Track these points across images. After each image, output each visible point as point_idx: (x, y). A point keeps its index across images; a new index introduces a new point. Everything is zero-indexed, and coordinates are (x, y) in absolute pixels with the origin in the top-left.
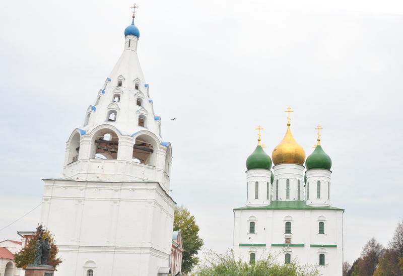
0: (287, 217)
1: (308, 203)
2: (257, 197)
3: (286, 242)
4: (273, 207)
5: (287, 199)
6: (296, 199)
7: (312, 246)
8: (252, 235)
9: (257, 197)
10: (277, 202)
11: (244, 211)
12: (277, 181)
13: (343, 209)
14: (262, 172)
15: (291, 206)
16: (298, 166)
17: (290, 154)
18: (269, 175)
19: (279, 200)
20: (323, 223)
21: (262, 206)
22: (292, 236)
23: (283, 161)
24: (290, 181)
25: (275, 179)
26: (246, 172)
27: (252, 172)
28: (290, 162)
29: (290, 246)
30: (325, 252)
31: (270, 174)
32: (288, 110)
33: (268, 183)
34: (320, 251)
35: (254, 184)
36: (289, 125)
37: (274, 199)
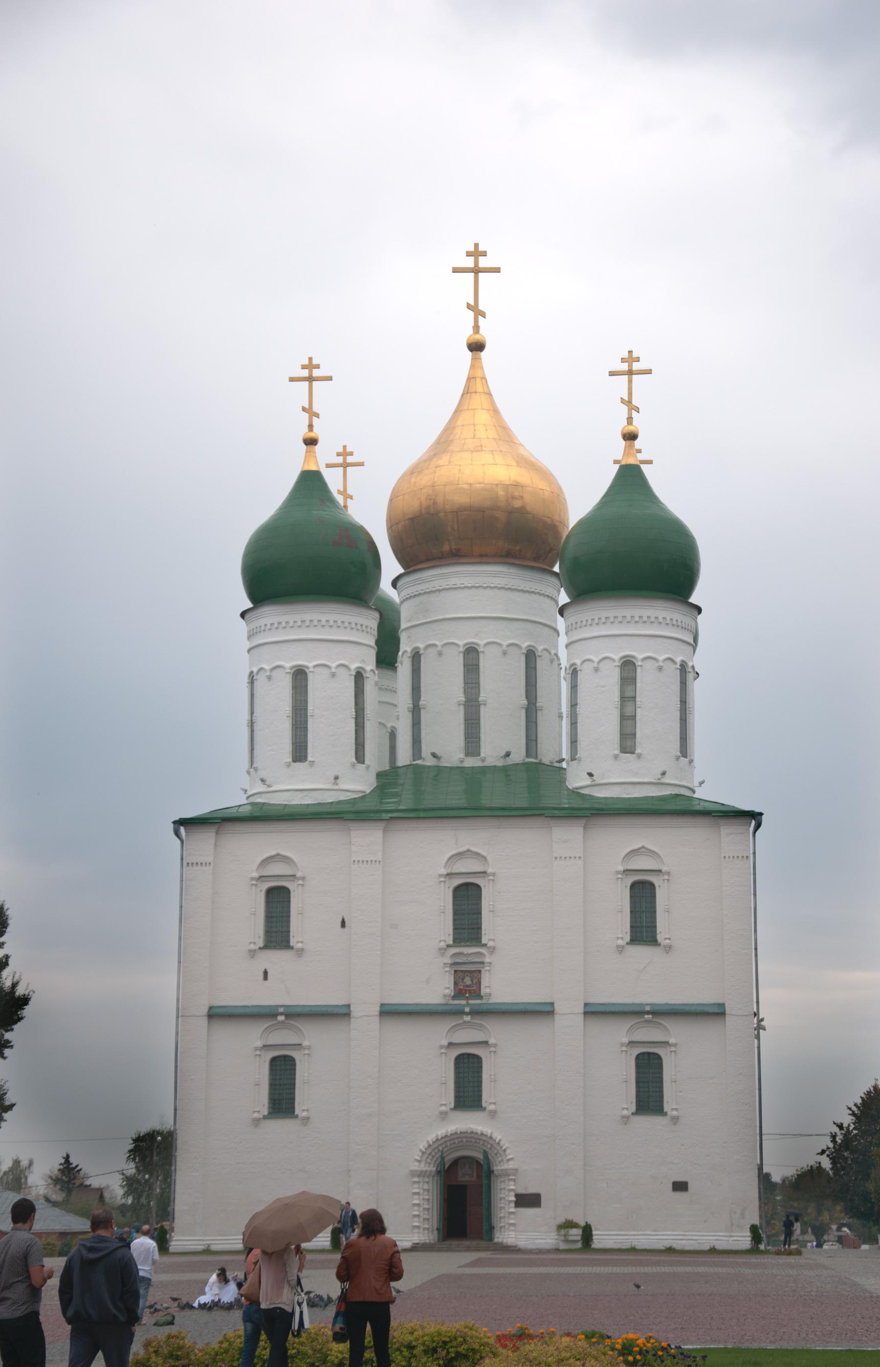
0: (460, 855)
1: (576, 780)
2: (300, 753)
3: (459, 993)
4: (390, 803)
5: (468, 754)
6: (519, 756)
7: (592, 1012)
8: (275, 959)
9: (300, 753)
10: (417, 771)
11: (229, 826)
12: (416, 657)
13: (757, 810)
14: (324, 618)
15: (492, 796)
16: (528, 574)
17: (481, 510)
18: (362, 629)
19: (430, 762)
20: (652, 886)
21: (329, 798)
22: (487, 960)
23: (446, 548)
24: (481, 656)
25: (406, 647)
26: (243, 615)
27: (271, 615)
28: (483, 558)
29: (475, 1013)
30: (666, 1043)
31: (370, 620)
32: (470, 262)
33: (359, 677)
34: (639, 1036)
35: (284, 685)
36: (477, 347)
37: (404, 757)
